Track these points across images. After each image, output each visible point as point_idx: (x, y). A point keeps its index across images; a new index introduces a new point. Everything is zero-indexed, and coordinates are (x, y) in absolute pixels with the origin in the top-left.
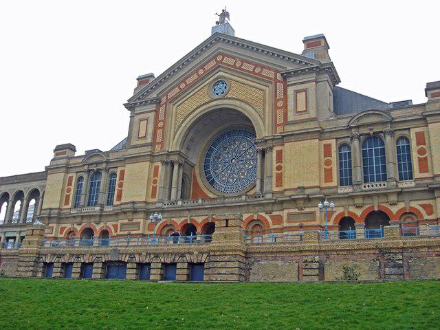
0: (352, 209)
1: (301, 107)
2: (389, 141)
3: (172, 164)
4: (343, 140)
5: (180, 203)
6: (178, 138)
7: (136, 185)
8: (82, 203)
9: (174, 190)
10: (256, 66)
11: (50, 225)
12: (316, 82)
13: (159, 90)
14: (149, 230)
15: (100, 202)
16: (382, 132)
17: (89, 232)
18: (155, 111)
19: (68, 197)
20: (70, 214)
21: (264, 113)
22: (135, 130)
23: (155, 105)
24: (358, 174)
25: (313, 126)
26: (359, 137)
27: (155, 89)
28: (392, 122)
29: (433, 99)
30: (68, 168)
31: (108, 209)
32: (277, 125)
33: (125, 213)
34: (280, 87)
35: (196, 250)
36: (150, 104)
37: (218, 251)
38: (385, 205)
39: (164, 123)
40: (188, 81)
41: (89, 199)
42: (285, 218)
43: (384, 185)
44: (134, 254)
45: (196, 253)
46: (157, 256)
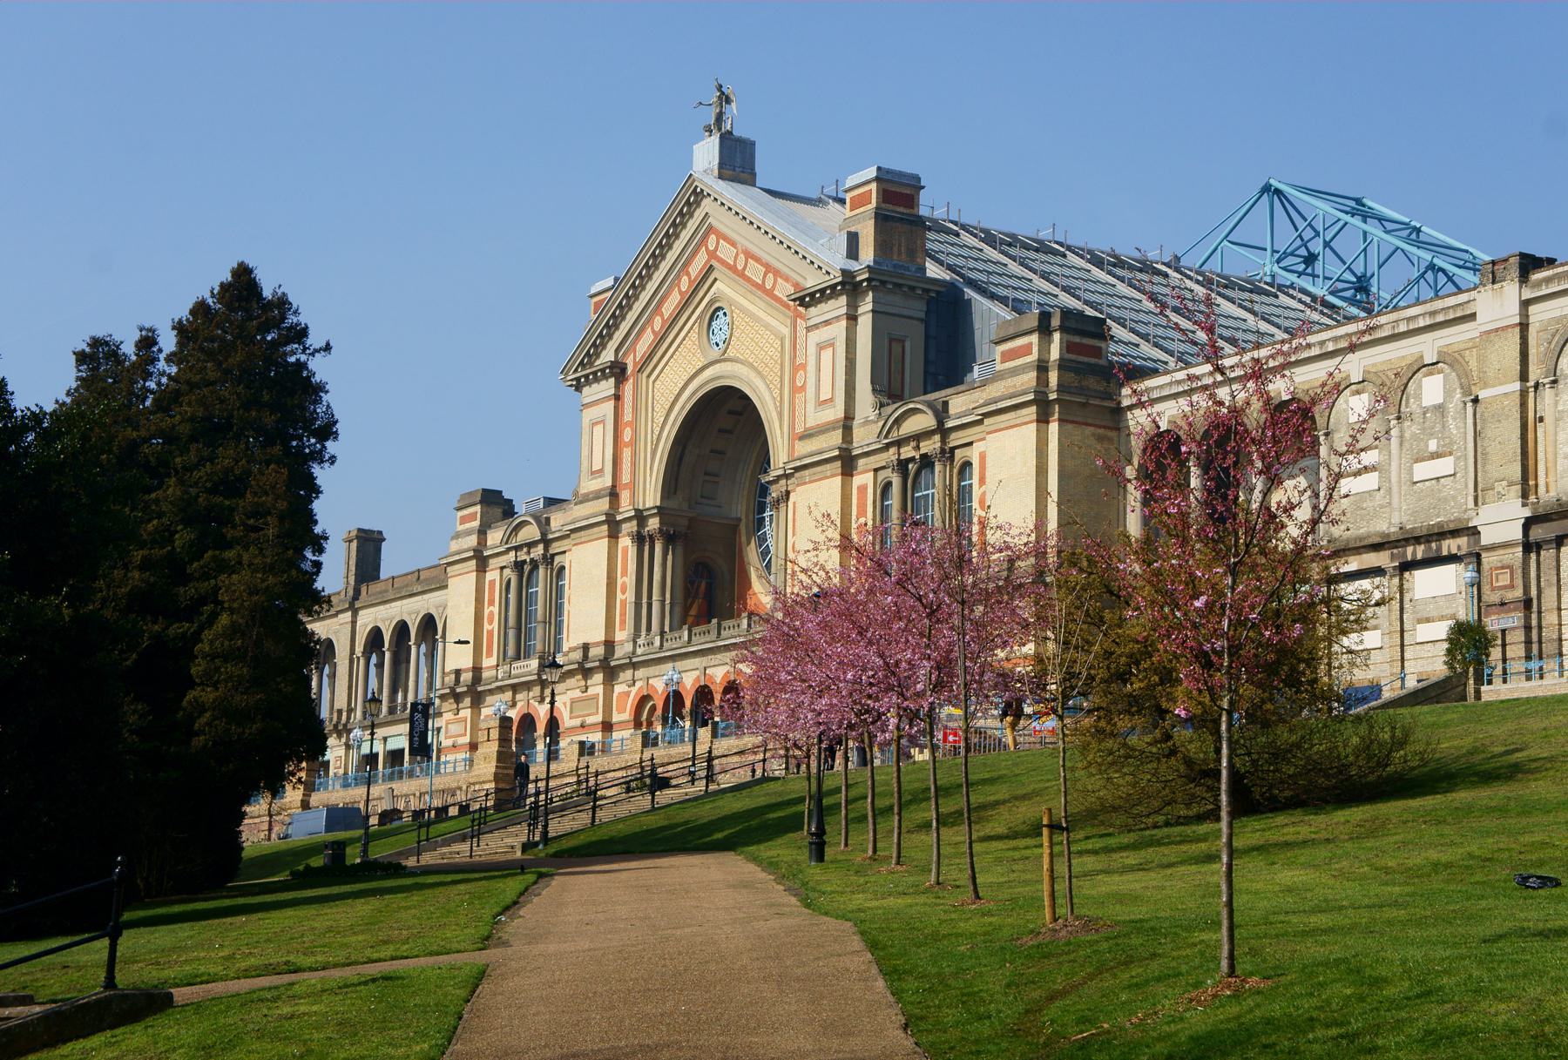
10: (769, 268)
13: (612, 345)
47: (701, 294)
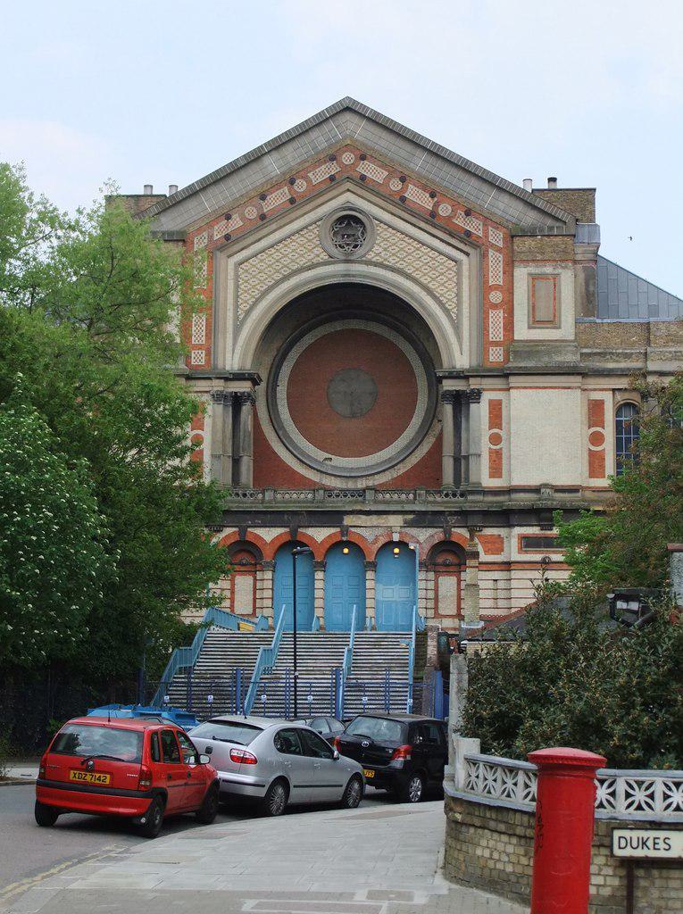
4: (627, 395)
6: (247, 344)
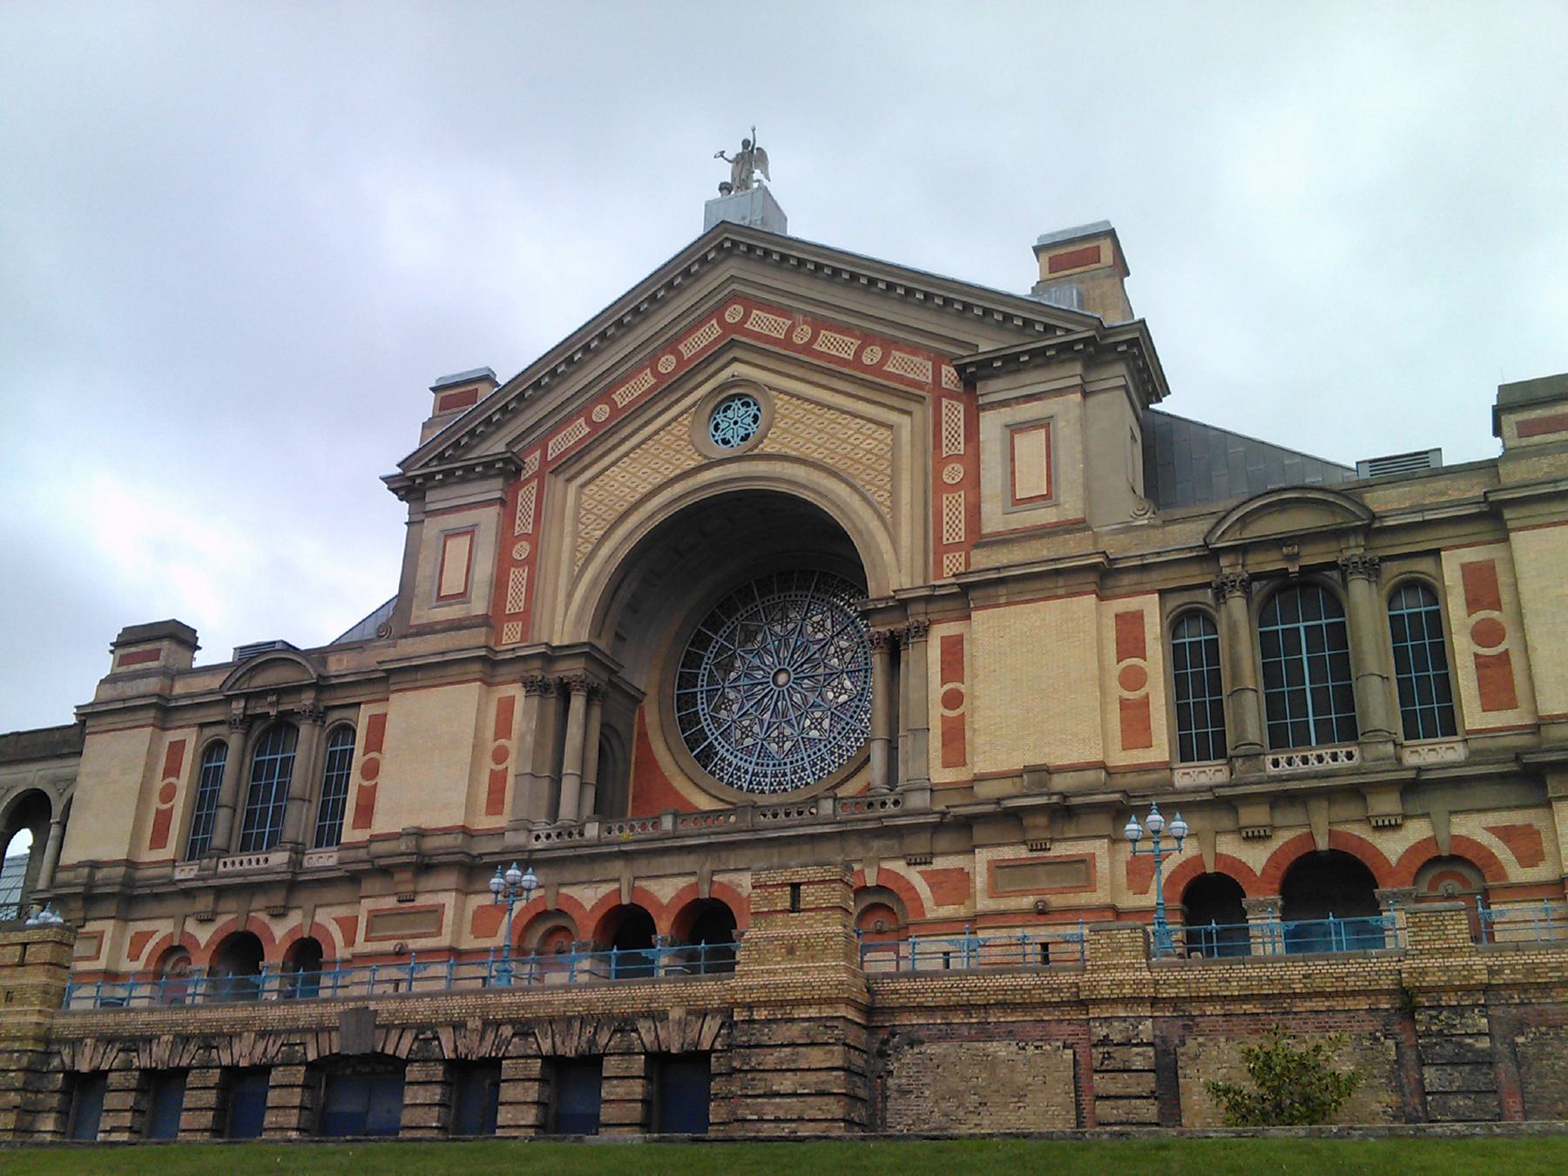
0: (1230, 847)
1: (1031, 481)
2: (1366, 607)
3: (564, 691)
4: (1185, 598)
5: (592, 831)
6: (586, 599)
7: (433, 765)
8: (218, 840)
9: (569, 787)
11: (92, 927)
12: (1085, 395)
14: (477, 932)
15: (289, 833)
16: (1333, 565)
17: (242, 950)
18: (502, 502)
19: (163, 819)
20: (173, 882)
21: (895, 507)
22: (426, 570)
23: (498, 483)
24: (1248, 717)
25: (1073, 548)
26: (1246, 586)
27: (500, 425)
28: (1371, 528)
29: (1525, 441)
30: (164, 711)
31: (323, 859)
32: (942, 549)
33: (386, 872)
34: (954, 413)
35: (681, 1000)
36: (483, 477)
37: (765, 1004)
38: (1358, 830)
39: (535, 547)
40: (622, 397)
41: (248, 824)
42: (980, 881)
43: (1350, 756)
44: (432, 1026)
45: (676, 1014)
46: (524, 1029)
47: (700, 378)
